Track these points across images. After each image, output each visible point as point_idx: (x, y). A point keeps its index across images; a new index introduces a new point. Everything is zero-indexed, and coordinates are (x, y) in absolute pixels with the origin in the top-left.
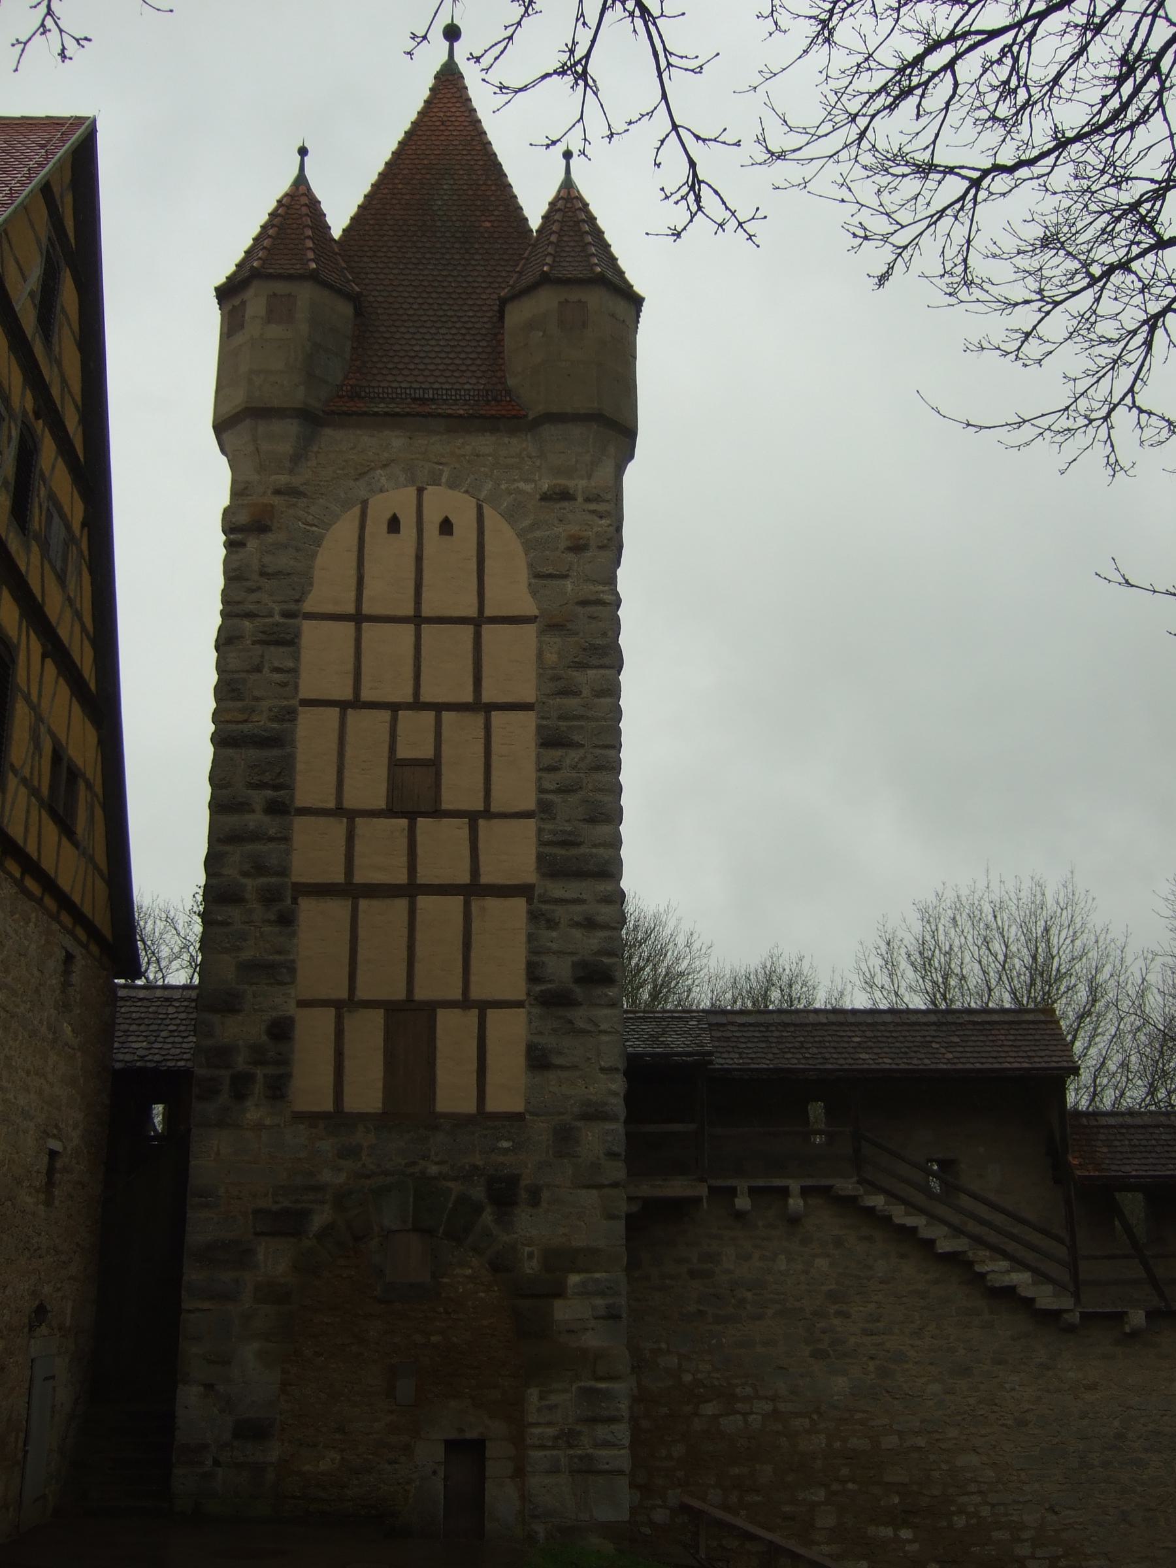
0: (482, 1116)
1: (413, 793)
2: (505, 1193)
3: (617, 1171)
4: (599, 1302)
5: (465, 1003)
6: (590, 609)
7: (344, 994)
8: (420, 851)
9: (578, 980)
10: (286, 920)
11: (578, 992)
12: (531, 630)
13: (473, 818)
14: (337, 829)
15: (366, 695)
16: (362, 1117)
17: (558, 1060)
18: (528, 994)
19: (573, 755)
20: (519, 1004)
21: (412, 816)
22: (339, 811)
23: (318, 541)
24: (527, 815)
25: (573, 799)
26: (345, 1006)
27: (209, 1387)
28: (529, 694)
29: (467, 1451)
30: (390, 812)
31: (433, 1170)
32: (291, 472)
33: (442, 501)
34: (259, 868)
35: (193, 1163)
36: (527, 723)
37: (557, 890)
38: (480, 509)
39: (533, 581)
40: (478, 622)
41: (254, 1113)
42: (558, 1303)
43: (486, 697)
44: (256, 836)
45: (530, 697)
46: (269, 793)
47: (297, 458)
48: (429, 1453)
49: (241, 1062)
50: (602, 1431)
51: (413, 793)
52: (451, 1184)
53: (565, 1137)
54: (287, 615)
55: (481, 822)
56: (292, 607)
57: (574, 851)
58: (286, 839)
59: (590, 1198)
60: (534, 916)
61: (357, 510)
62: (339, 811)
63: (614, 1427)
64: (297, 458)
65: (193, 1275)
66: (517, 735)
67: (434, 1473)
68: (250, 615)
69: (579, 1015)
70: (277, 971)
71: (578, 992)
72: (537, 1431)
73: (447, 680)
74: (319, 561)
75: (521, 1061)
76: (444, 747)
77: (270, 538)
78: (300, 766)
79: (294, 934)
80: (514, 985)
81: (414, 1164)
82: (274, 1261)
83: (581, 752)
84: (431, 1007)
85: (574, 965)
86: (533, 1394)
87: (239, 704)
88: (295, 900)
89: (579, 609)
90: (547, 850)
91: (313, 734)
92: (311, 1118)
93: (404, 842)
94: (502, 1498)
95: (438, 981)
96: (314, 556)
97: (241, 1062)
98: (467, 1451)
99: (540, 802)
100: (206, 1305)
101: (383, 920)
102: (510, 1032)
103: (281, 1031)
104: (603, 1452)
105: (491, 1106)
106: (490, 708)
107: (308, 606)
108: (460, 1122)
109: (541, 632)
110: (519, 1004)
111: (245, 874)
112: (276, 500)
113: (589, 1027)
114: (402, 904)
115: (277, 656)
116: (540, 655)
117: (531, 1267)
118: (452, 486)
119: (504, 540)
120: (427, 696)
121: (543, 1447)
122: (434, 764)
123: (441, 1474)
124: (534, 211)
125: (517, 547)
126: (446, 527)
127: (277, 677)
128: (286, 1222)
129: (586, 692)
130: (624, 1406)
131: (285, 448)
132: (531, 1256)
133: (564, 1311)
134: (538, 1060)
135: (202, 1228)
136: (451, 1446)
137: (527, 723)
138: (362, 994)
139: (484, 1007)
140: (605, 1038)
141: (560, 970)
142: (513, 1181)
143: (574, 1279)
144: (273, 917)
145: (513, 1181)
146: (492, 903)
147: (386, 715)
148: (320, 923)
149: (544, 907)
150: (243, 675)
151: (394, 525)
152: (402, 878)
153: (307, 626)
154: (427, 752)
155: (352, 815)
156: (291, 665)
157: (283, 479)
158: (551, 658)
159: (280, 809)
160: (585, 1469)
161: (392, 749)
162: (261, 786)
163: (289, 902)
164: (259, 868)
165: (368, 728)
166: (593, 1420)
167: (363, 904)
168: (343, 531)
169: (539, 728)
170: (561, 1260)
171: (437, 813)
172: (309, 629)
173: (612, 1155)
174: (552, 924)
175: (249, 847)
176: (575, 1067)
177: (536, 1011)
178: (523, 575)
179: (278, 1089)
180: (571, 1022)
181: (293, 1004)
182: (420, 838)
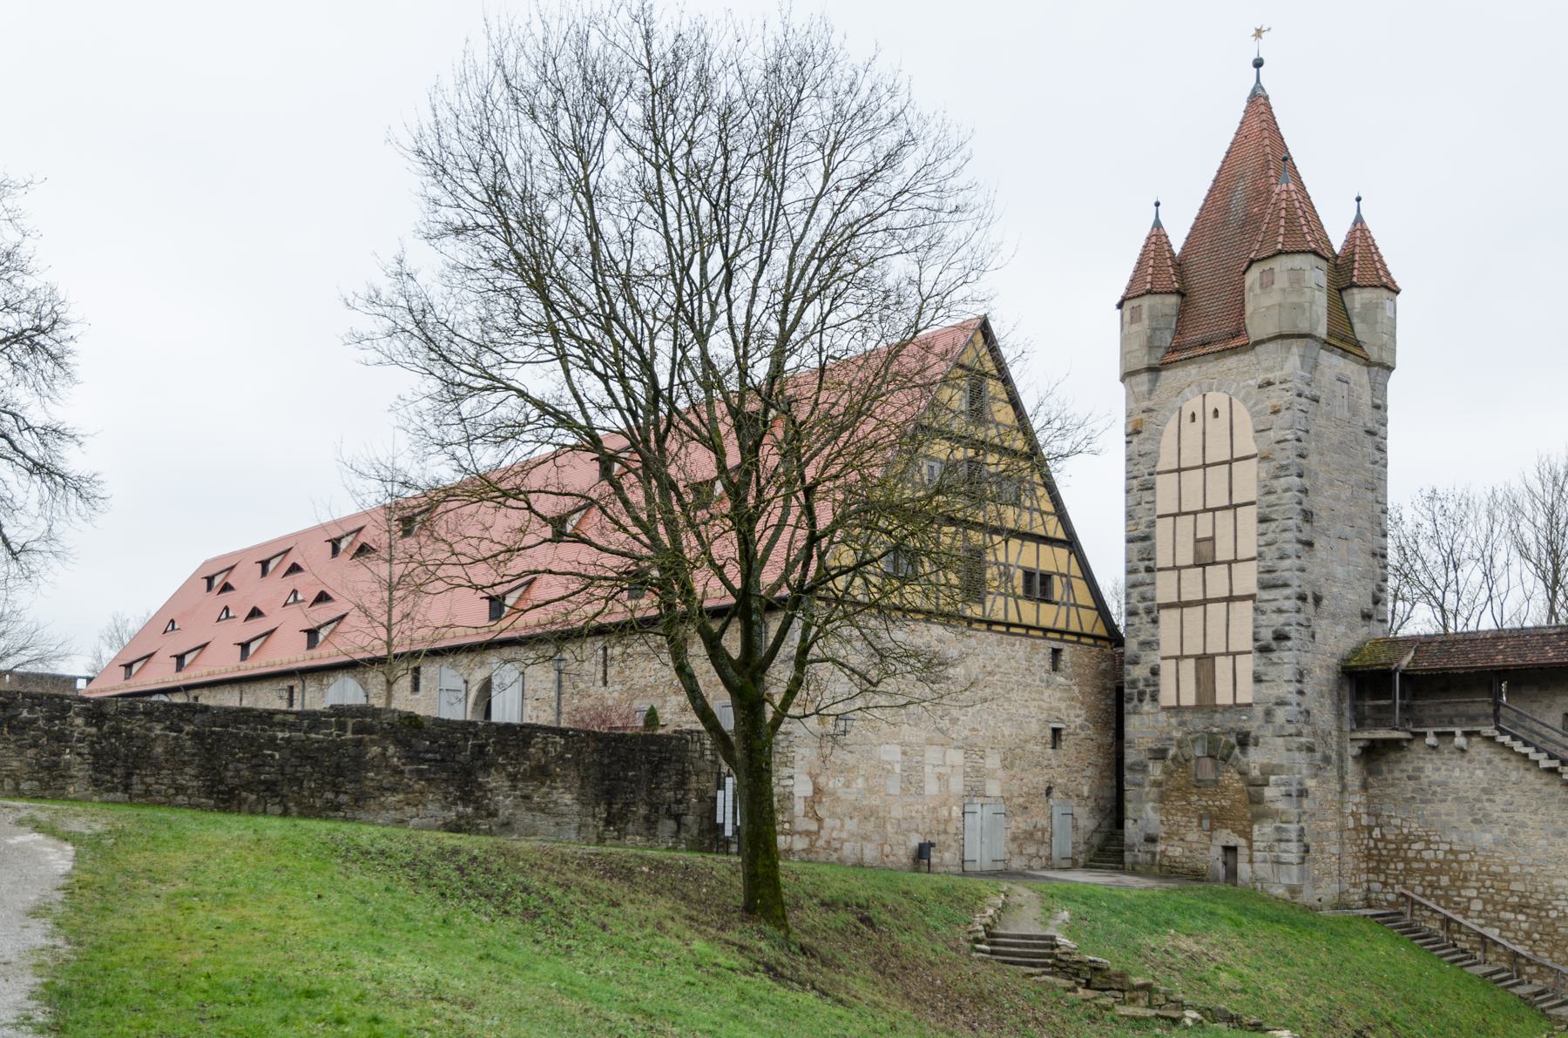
0: (1236, 707)
5: (1227, 654)
11: (1274, 645)
13: (1229, 563)
14: (1174, 575)
21: (1203, 566)
22: (1175, 568)
30: (1196, 565)
33: (1217, 399)
37: (1265, 595)
47: (1151, 391)
50: (1283, 845)
53: (1268, 714)
59: (1280, 741)
60: (1256, 609)
62: (1175, 568)
64: (1151, 391)
69: (1274, 656)
70: (1149, 645)
71: (1274, 645)
75: (1250, 679)
77: (1142, 436)
80: (1249, 645)
84: (1213, 656)
85: (1274, 632)
86: (1256, 827)
91: (1163, 530)
94: (1243, 869)
98: (1230, 850)
102: (1247, 665)
107: (1158, 469)
108: (1226, 708)
112: (1144, 416)
114: (1201, 608)
115: (1147, 496)
117: (1255, 773)
122: (1212, 539)
131: (1145, 388)
133: (1269, 792)
134: (1258, 679)
139: (1234, 654)
141: (1267, 635)
143: (1272, 778)
145: (1247, 735)
148: (1168, 618)
152: (1201, 597)
153: (1158, 478)
154: (1209, 534)
157: (1146, 404)
160: (1278, 862)
165: (1185, 523)
166: (1280, 840)
168: (1172, 426)
170: (1267, 771)
171: (1214, 563)
172: (1159, 479)
174: (1263, 613)
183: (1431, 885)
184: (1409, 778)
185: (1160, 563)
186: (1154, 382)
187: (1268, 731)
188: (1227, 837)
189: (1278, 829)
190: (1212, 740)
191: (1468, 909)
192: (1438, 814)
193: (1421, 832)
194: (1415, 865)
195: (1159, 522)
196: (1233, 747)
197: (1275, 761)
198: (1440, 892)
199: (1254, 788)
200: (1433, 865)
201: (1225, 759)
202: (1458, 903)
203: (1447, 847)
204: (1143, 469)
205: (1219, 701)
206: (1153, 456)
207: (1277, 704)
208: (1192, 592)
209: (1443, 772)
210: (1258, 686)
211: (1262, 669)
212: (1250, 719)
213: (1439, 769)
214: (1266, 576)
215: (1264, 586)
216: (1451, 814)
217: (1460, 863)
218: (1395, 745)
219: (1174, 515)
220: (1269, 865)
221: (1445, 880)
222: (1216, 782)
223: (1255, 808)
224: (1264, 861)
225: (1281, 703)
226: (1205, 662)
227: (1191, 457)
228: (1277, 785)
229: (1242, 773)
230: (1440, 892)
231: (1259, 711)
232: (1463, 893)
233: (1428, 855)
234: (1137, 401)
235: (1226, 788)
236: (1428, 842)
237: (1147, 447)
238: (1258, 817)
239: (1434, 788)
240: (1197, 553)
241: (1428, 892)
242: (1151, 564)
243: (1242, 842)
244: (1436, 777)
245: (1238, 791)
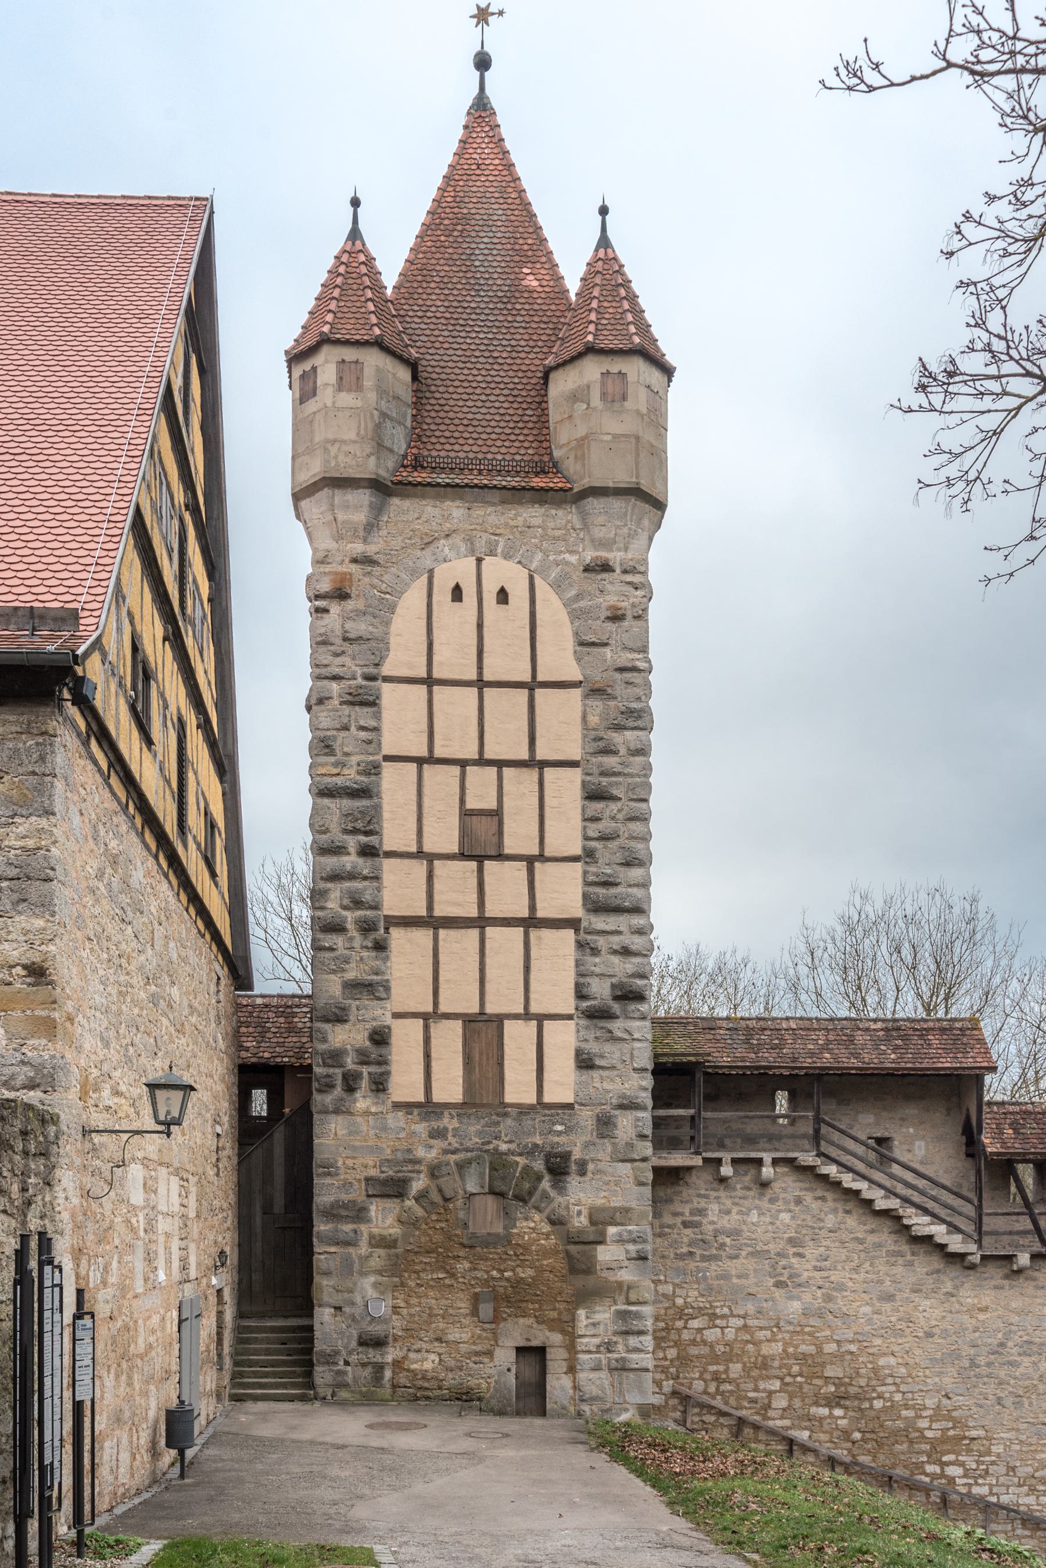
1: (481, 842)
3: (646, 1148)
4: (631, 1247)
5: (527, 1015)
6: (628, 676)
7: (430, 1009)
8: (487, 889)
9: (616, 998)
10: (380, 947)
11: (616, 1007)
12: (577, 693)
13: (530, 861)
14: (420, 868)
15: (439, 753)
16: (447, 1106)
17: (598, 1062)
18: (577, 1009)
19: (614, 807)
20: (570, 1017)
21: (481, 859)
22: (420, 854)
23: (392, 609)
24: (575, 859)
25: (613, 845)
27: (338, 1308)
28: (575, 753)
29: (534, 1355)
30: (463, 856)
31: (504, 1147)
32: (365, 541)
34: (357, 903)
35: (316, 1141)
36: (574, 778)
37: (600, 922)
38: (531, 578)
39: (578, 648)
40: (532, 686)
41: (363, 1102)
42: (600, 1248)
43: (540, 756)
44: (352, 876)
45: (577, 757)
46: (363, 839)
47: (370, 527)
48: (505, 1356)
50: (633, 1341)
51: (481, 842)
52: (518, 1159)
54: (371, 678)
55: (537, 865)
56: (372, 670)
57: (613, 891)
58: (377, 878)
59: (625, 1169)
60: (580, 945)
61: (424, 578)
63: (642, 1338)
64: (370, 527)
65: (321, 1227)
66: (566, 788)
67: (509, 1370)
68: (336, 678)
69: (617, 1026)
71: (616, 1007)
72: (585, 1340)
73: (507, 740)
74: (393, 628)
75: (571, 1063)
76: (505, 799)
77: (350, 605)
78: (386, 815)
79: (387, 958)
80: (567, 1004)
81: (489, 1143)
82: (384, 1218)
83: (619, 804)
84: (499, 1020)
85: (613, 986)
86: (581, 1313)
87: (332, 759)
88: (387, 929)
89: (618, 676)
90: (592, 889)
91: (395, 786)
92: (407, 1107)
93: (474, 881)
94: (559, 1386)
95: (504, 999)
96: (387, 623)
98: (534, 1355)
99: (584, 849)
100: (333, 1249)
101: (459, 945)
102: (563, 1039)
103: (380, 1038)
104: (634, 1356)
105: (547, 1099)
106: (543, 765)
107: (386, 670)
108: (524, 1110)
109: (586, 696)
110: (570, 1017)
111: (345, 908)
112: (354, 568)
113: (626, 1036)
114: (474, 933)
115: (363, 716)
116: (584, 718)
117: (580, 1222)
118: (507, 557)
119: (552, 609)
120: (489, 755)
121: (589, 1352)
122: (497, 814)
123: (514, 1371)
125: (564, 616)
126: (503, 596)
127: (363, 735)
128: (393, 1188)
129: (623, 751)
130: (649, 1324)
132: (579, 1213)
133: (605, 1254)
134: (585, 1063)
135: (326, 1192)
136: (520, 1350)
137: (574, 778)
138: (443, 1008)
139: (541, 1019)
140: (637, 1045)
141: (601, 990)
142: (566, 1156)
143: (612, 1230)
144: (370, 945)
146: (546, 934)
147: (456, 770)
148: (408, 950)
149: (589, 937)
150: (334, 733)
151: (457, 593)
152: (474, 913)
153: (386, 688)
154: (493, 805)
155: (431, 858)
156: (373, 723)
157: (358, 548)
158: (594, 720)
159: (368, 852)
161: (462, 801)
162: (354, 831)
163: (382, 931)
164: (357, 903)
165: (441, 782)
166: (627, 1333)
167: (442, 933)
168: (413, 600)
169: (584, 784)
171: (501, 857)
172: (389, 693)
173: (642, 1137)
174: (595, 952)
175: (347, 884)
176: (614, 1068)
177: (584, 1022)
178: (569, 643)
179: (380, 1086)
180: (610, 1032)
181: (389, 1015)
182: (487, 878)
183: (716, 1378)
184: (686, 1225)
185: (389, 844)
186: (378, 510)
187: (604, 1151)
188: (518, 1332)
189: (622, 1315)
190: (499, 1164)
191: (768, 1406)
192: (725, 1277)
193: (702, 1302)
194: (694, 1351)
195: (388, 769)
196: (539, 1178)
197: (617, 1202)
198: (728, 1387)
199: (577, 1250)
200: (720, 1349)
201: (522, 1198)
202: (754, 1401)
203: (740, 1322)
204: (352, 665)
205: (509, 1098)
206: (376, 647)
207: (621, 1107)
209: (734, 1216)
210: (586, 1075)
211: (593, 1047)
212: (569, 1130)
213: (728, 1212)
214: (601, 891)
215: (596, 907)
216: (746, 1276)
217: (756, 1343)
219: (420, 761)
220: (604, 1375)
221: (736, 1369)
222: (507, 1240)
223: (579, 1281)
224: (597, 1368)
225: (628, 1105)
226: (483, 1030)
227: (454, 659)
228: (620, 1241)
229: (556, 1222)
230: (728, 1387)
231: (586, 1117)
232: (762, 1385)
233: (711, 1335)
234: (338, 537)
235: (526, 1248)
236: (713, 1316)
237: (359, 627)
238: (586, 1297)
239: (722, 1238)
240: (465, 833)
241: (712, 1389)
242: (372, 840)
243: (556, 1338)
244: (724, 1223)
245: (545, 1253)
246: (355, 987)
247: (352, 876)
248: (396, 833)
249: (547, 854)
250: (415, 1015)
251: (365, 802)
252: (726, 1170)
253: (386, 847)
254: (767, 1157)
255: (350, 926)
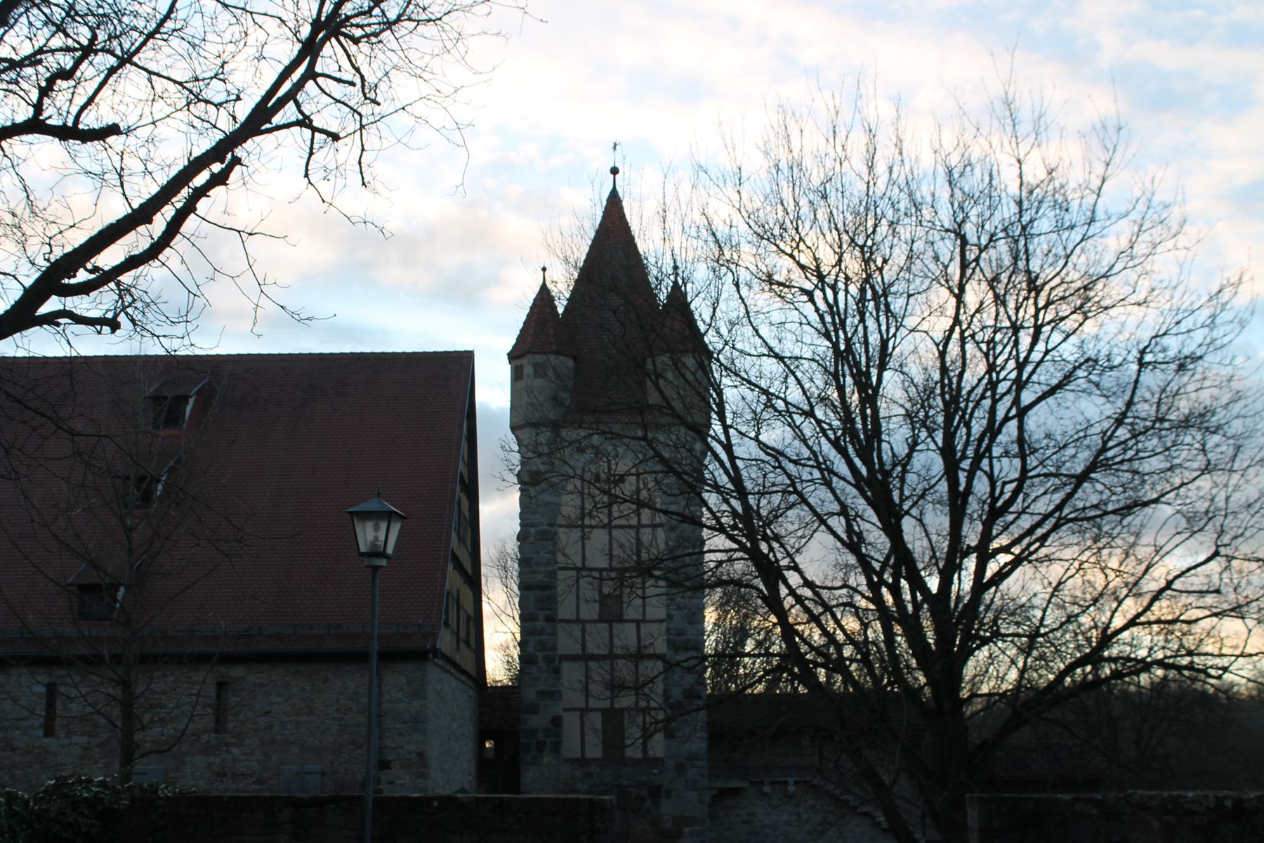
2: (656, 792)
10: (557, 671)
14: (576, 630)
26: (584, 711)
30: (601, 620)
31: (625, 783)
34: (543, 646)
41: (547, 759)
44: (541, 633)
49: (540, 736)
57: (684, 638)
62: (578, 620)
68: (533, 526)
92: (572, 761)
97: (540, 736)
103: (557, 721)
108: (636, 762)
117: (669, 825)
124: (662, 297)
143: (687, 829)
148: (572, 673)
155: (584, 622)
159: (550, 619)
172: (562, 534)
175: (538, 638)
179: (556, 748)
208: (597, 646)
218: (735, 792)
246: (543, 694)
247: (541, 633)
248: (566, 609)
249: (648, 618)
250: (575, 710)
251: (548, 592)
252: (767, 789)
253: (560, 617)
254: (791, 781)
255: (540, 660)
